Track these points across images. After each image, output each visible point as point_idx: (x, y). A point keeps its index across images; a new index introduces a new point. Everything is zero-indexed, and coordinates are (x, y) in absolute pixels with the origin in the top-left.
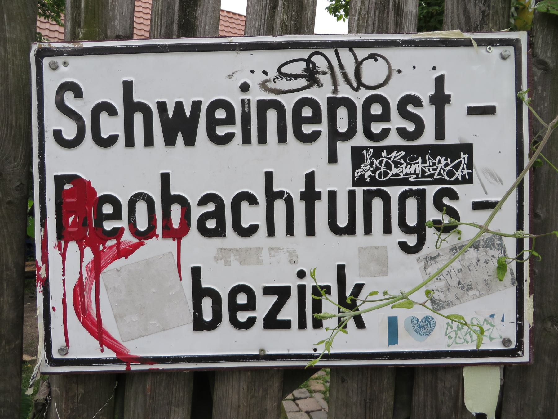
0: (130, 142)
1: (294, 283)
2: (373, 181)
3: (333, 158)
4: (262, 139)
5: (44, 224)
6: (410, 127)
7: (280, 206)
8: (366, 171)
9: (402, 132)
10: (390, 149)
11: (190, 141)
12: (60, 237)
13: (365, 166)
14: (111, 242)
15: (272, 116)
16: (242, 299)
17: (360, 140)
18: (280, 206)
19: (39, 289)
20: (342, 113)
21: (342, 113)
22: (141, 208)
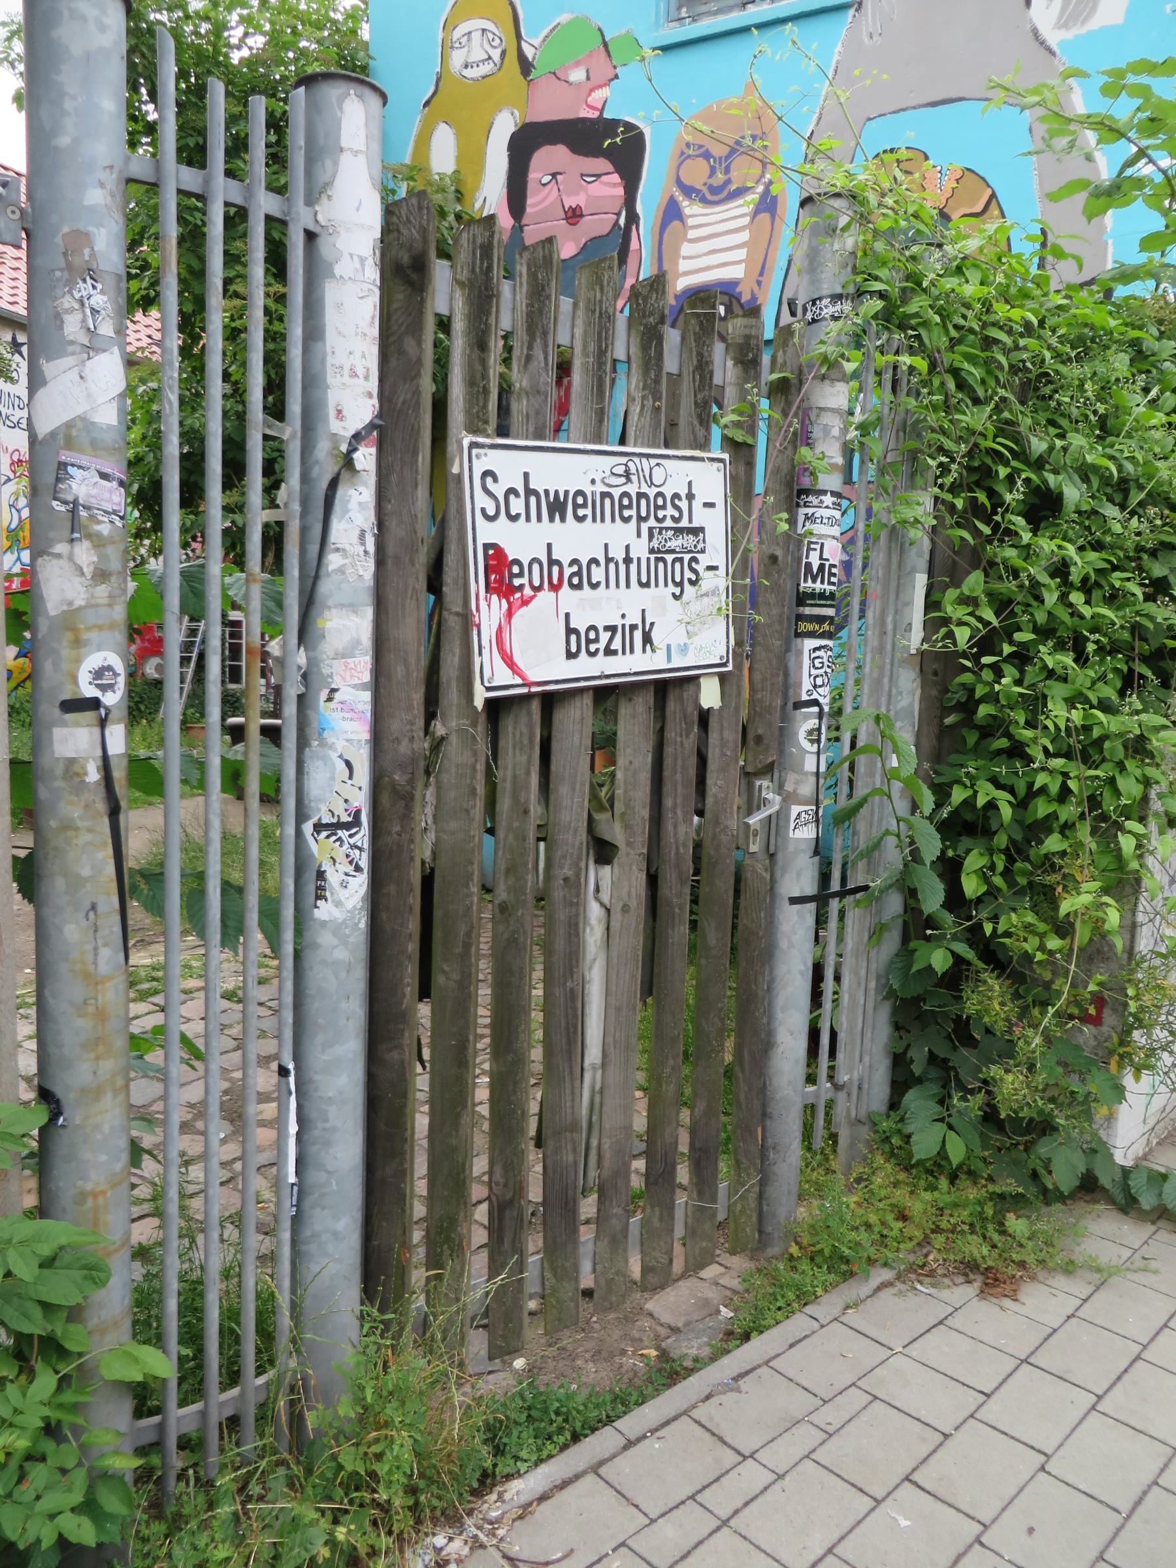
0: (528, 519)
1: (618, 622)
2: (659, 551)
3: (639, 535)
4: (603, 520)
7: (612, 566)
8: (655, 544)
9: (672, 517)
10: (667, 529)
11: (563, 519)
13: (655, 540)
14: (518, 595)
15: (607, 502)
16: (592, 635)
17: (652, 522)
18: (612, 566)
19: (475, 632)
20: (643, 502)
21: (643, 502)
22: (536, 567)
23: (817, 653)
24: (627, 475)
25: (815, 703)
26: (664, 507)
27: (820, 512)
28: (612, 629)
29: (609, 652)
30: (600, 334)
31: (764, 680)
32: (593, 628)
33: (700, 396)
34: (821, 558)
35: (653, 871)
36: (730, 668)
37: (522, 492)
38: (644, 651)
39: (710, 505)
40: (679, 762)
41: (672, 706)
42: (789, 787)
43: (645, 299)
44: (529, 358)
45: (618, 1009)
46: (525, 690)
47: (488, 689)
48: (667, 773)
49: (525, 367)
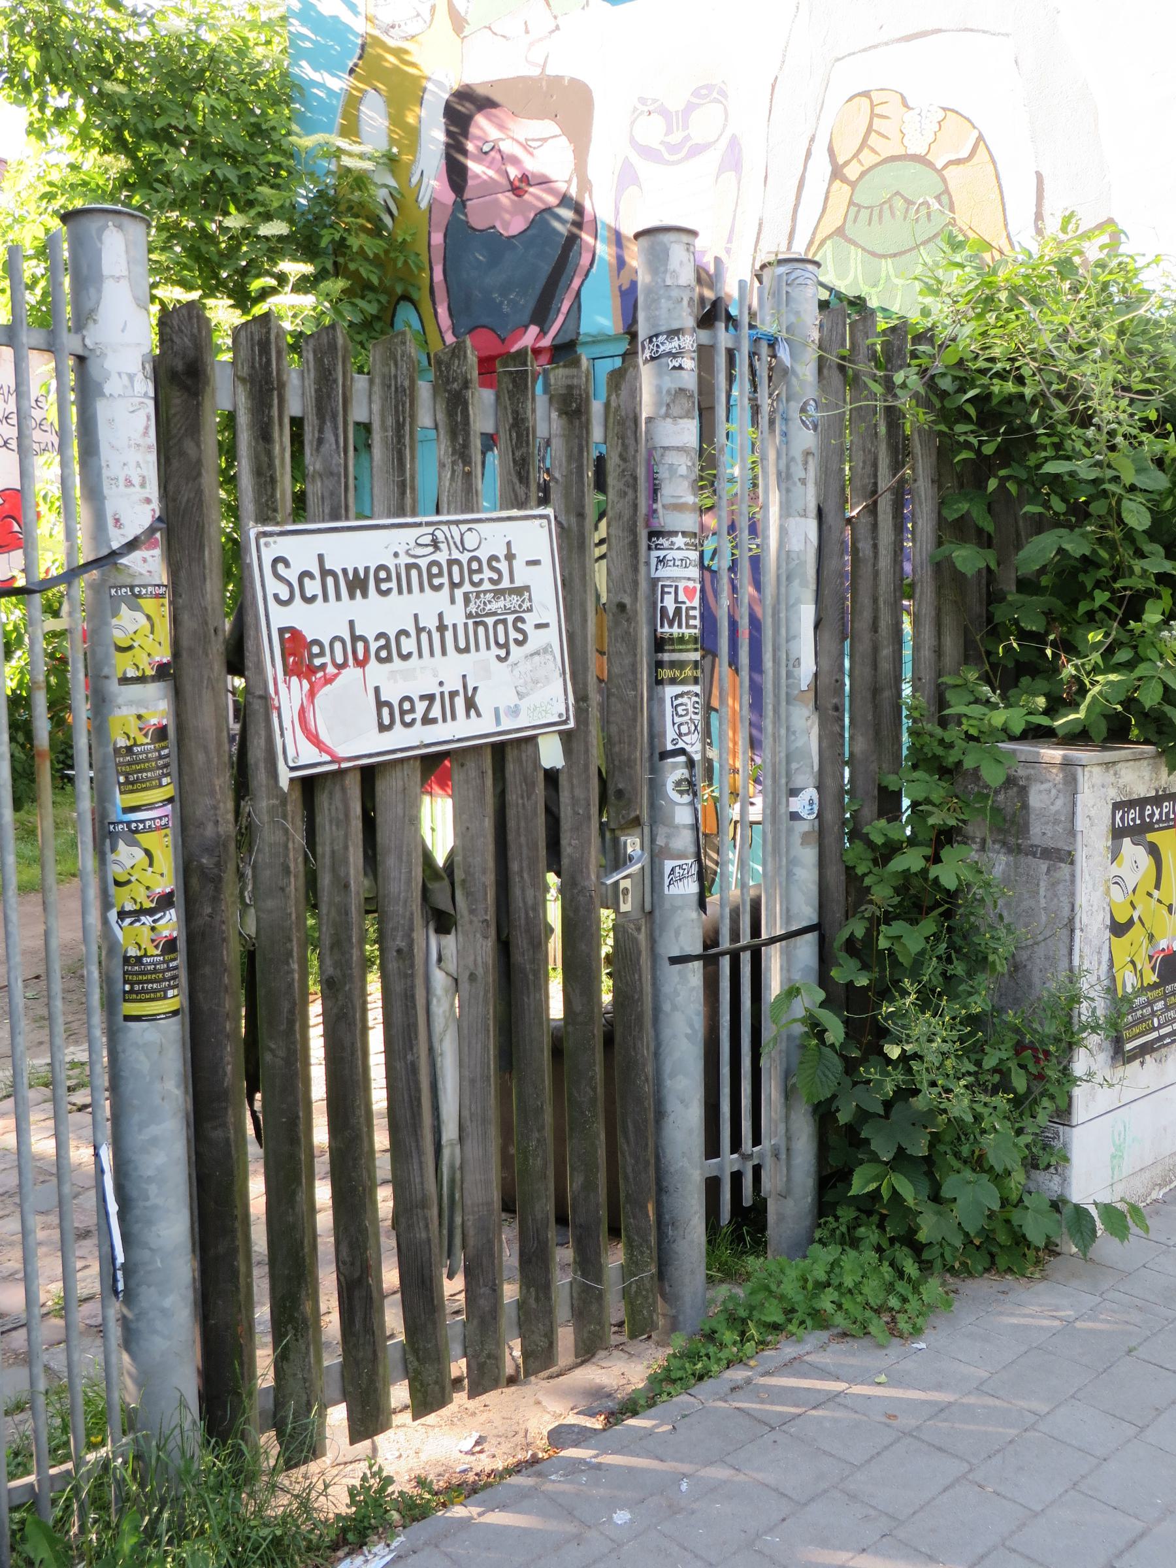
0: (326, 598)
1: (436, 690)
2: (478, 615)
3: (453, 601)
4: (410, 591)
5: (273, 666)
6: (495, 576)
7: (424, 636)
8: (472, 608)
9: (491, 580)
10: (485, 592)
11: (365, 595)
12: (285, 674)
15: (414, 573)
16: (407, 706)
17: (467, 587)
18: (424, 636)
20: (455, 569)
21: (455, 569)
22: (338, 646)
23: (680, 701)
24: (435, 544)
25: (682, 752)
26: (480, 571)
27: (671, 555)
28: (430, 698)
29: (427, 720)
30: (396, 407)
31: (621, 731)
32: (407, 698)
33: (518, 454)
34: (676, 601)
35: (504, 937)
36: (571, 724)
37: (317, 573)
38: (468, 715)
40: (523, 824)
41: (511, 767)
42: (660, 841)
43: (448, 367)
44: (320, 441)
45: (473, 1081)
46: (334, 767)
47: (292, 769)
48: (511, 837)
49: (318, 449)
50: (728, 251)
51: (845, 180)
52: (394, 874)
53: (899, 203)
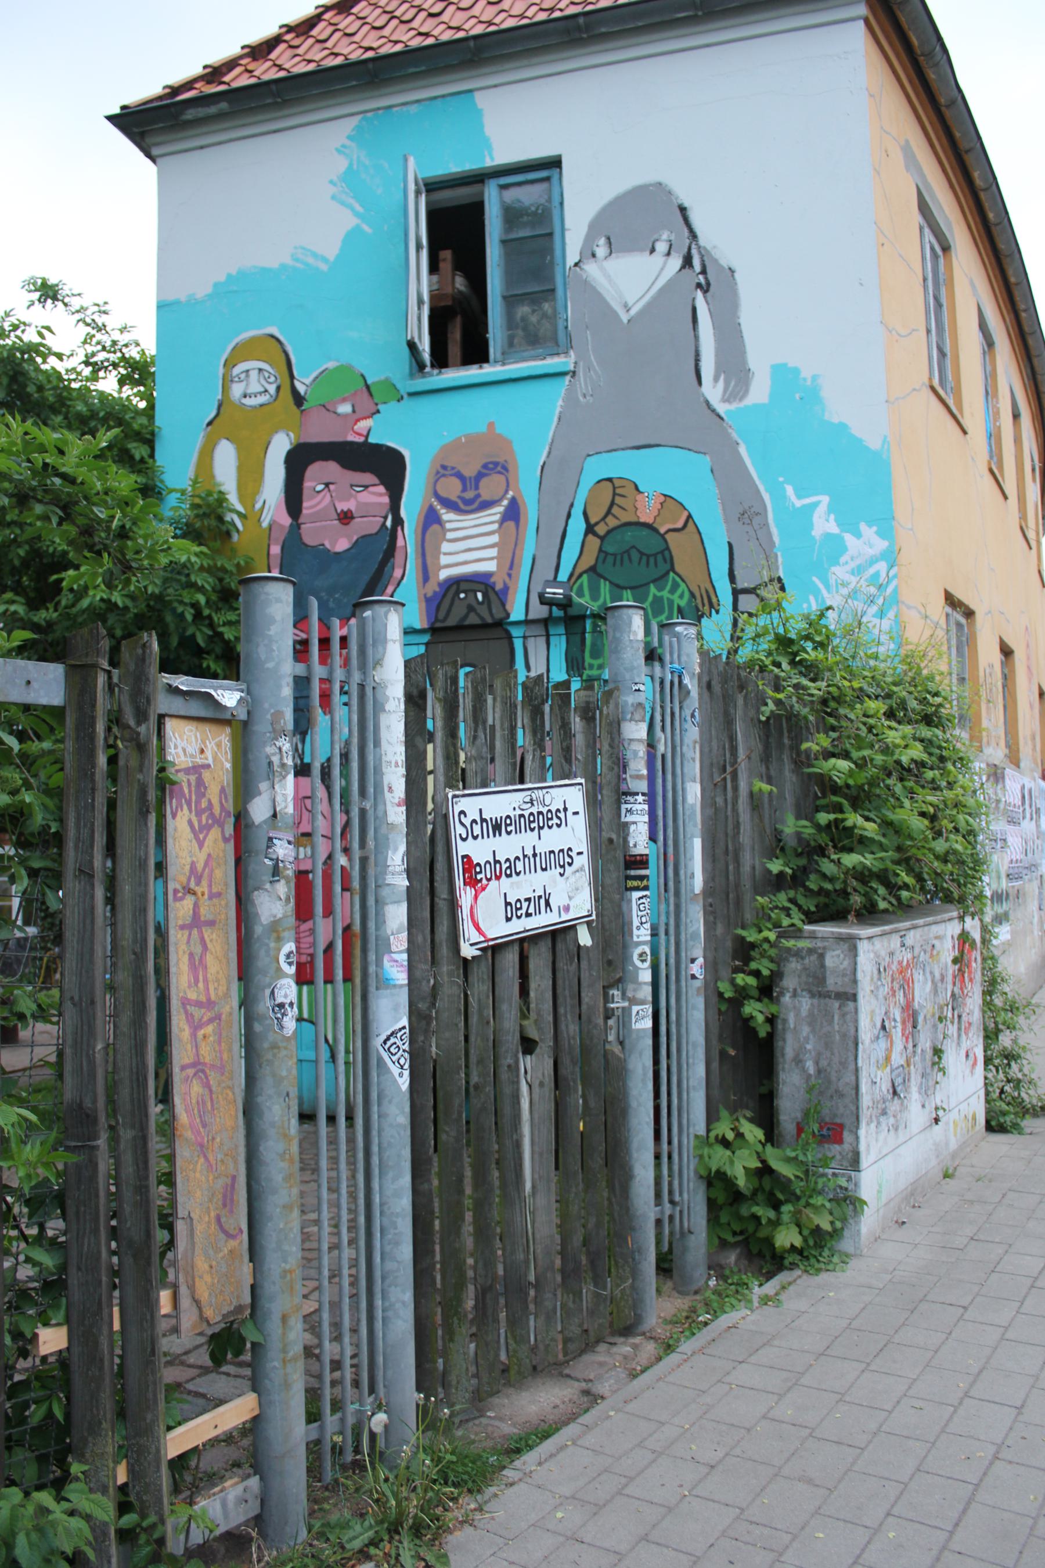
28: (528, 900)
29: (528, 915)
32: (519, 900)
39: (576, 813)
50: (510, 575)
51: (595, 534)
52: (507, 1015)
53: (635, 555)
